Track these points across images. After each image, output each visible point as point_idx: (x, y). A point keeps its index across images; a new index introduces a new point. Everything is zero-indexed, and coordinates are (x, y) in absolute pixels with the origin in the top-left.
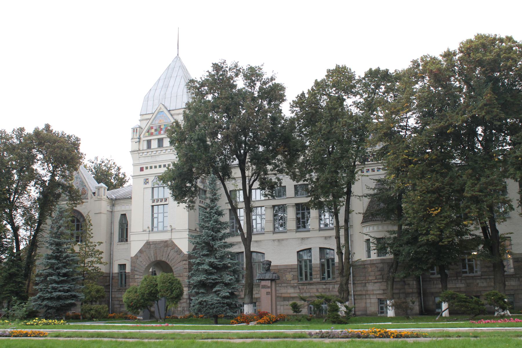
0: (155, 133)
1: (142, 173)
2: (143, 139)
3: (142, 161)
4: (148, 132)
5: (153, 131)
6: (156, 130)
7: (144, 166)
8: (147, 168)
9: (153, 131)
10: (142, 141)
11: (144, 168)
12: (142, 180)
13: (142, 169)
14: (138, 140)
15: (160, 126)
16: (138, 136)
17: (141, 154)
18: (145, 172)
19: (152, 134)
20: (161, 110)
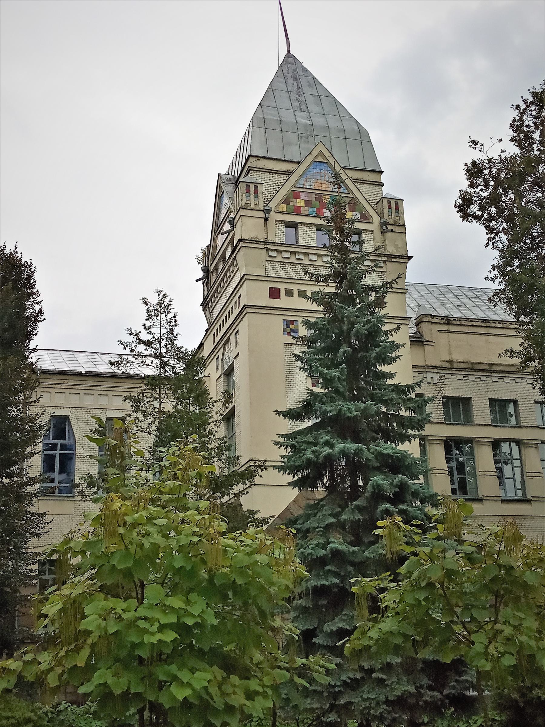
0: (306, 210)
1: (275, 303)
2: (273, 216)
3: (274, 271)
4: (286, 201)
5: (300, 203)
6: (308, 203)
7: (283, 287)
8: (289, 293)
9: (300, 203)
10: (271, 222)
11: (282, 293)
12: (278, 322)
13: (274, 293)
14: (262, 215)
15: (319, 197)
16: (261, 206)
17: (274, 254)
18: (284, 302)
19: (297, 211)
20: (320, 159)
